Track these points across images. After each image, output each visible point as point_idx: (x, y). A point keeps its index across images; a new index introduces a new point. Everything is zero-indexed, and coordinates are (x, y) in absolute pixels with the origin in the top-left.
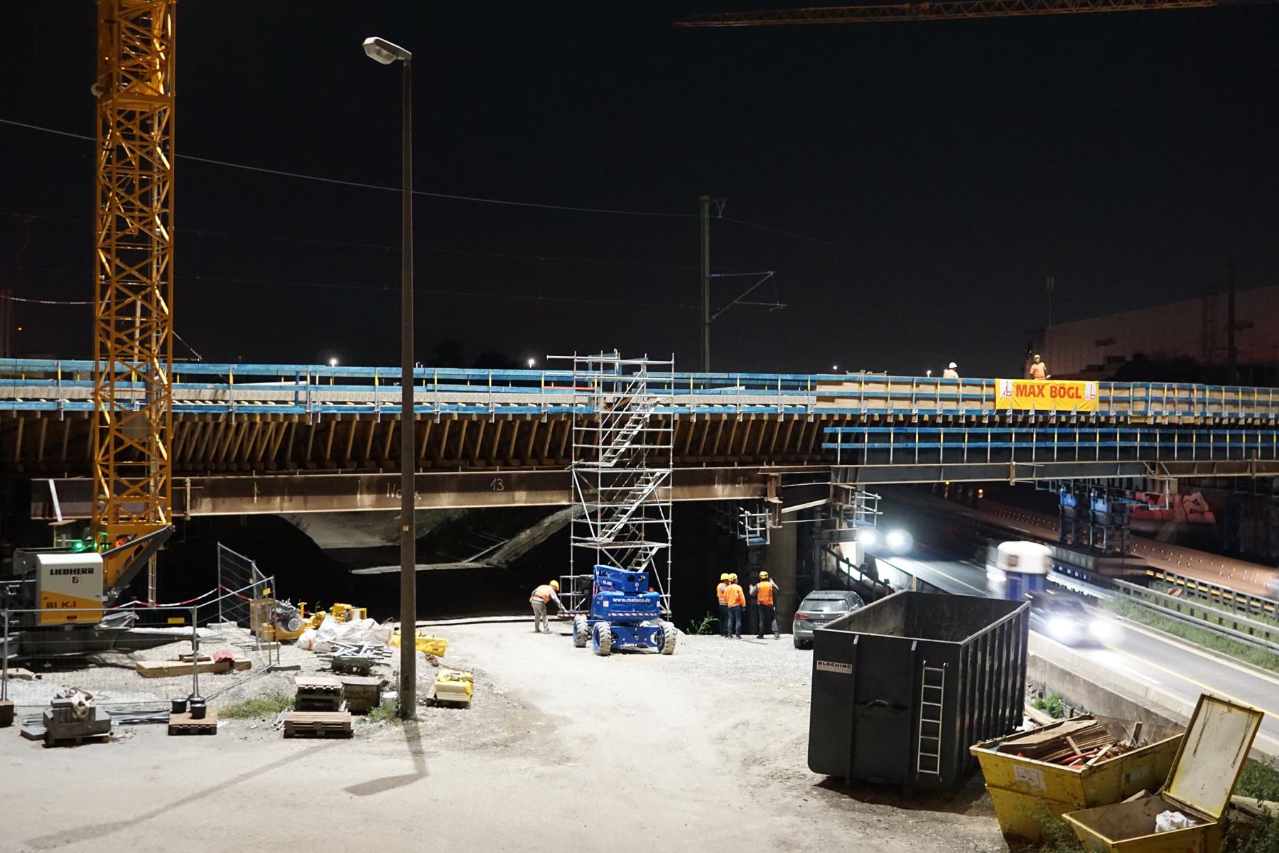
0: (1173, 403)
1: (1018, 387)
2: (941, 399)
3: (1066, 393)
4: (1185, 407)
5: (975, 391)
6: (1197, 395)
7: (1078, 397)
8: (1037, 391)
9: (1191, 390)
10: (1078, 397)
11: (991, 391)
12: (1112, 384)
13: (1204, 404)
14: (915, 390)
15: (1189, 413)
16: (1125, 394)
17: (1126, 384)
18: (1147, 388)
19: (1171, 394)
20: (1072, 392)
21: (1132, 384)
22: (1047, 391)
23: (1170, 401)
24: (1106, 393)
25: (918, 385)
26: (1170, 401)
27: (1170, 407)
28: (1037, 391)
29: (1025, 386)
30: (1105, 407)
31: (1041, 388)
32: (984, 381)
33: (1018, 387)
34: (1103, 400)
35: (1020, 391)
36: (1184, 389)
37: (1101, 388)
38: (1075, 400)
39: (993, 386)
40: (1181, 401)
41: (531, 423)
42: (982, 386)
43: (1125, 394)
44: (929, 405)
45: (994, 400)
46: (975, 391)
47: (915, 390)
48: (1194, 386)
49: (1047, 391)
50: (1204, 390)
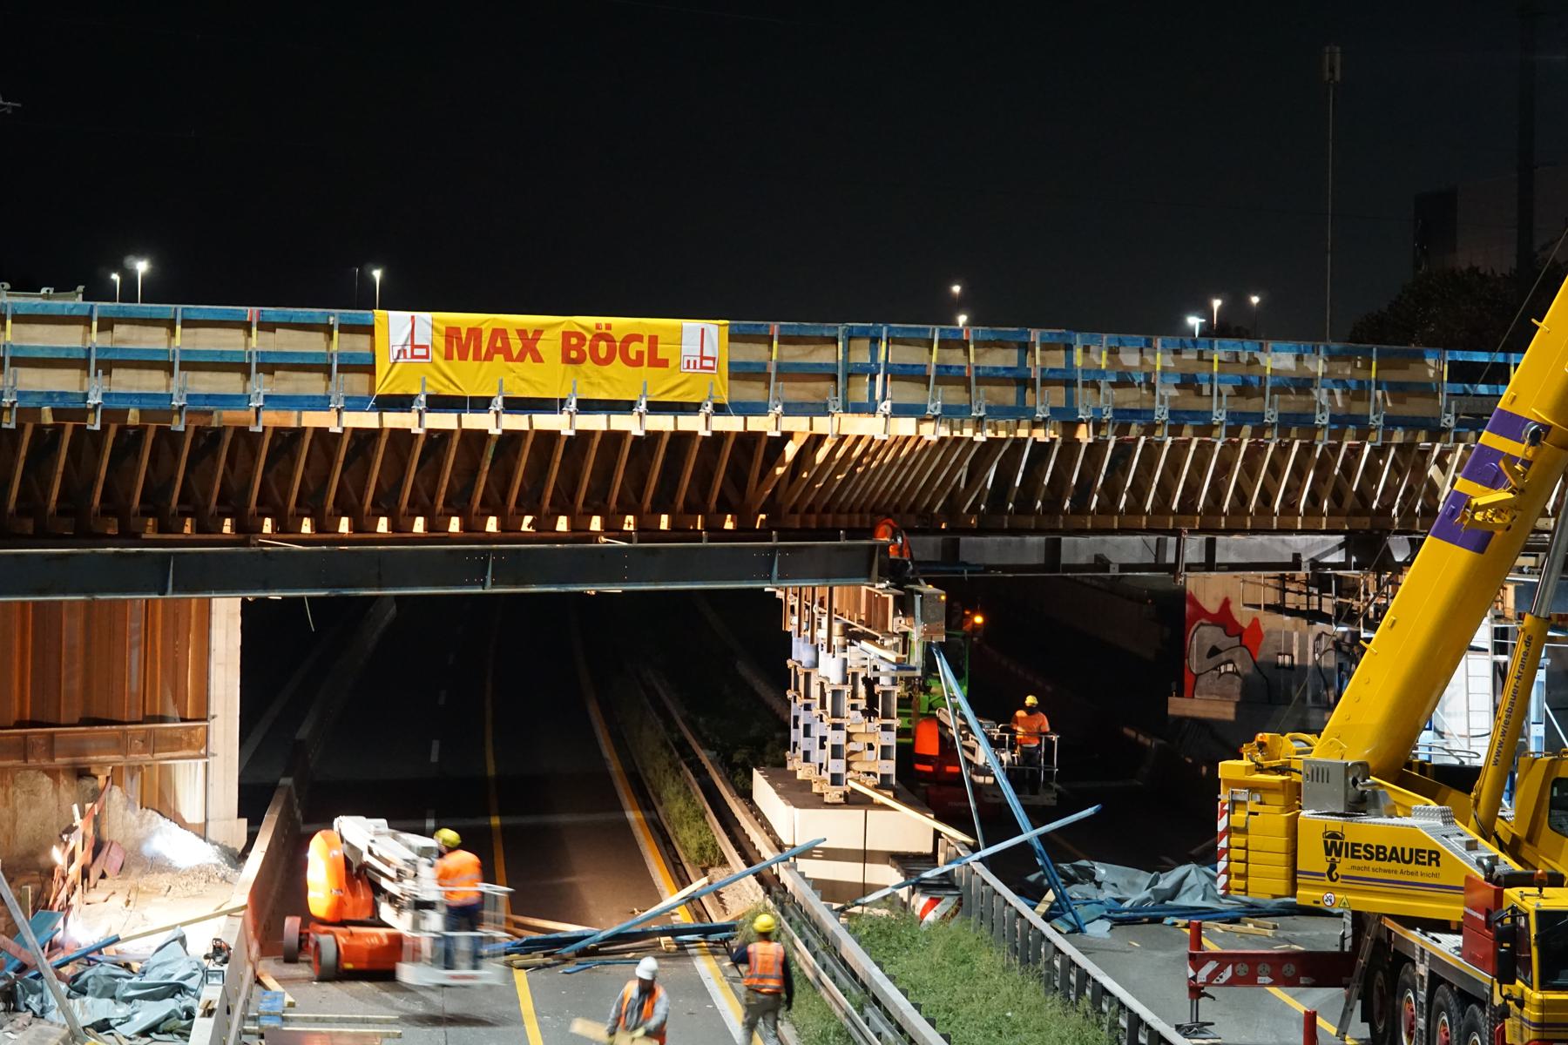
0: (965, 382)
1: (452, 334)
2: (185, 366)
3: (619, 350)
4: (1009, 395)
5: (312, 343)
6: (1038, 361)
7: (664, 363)
8: (516, 345)
9: (1026, 347)
10: (664, 363)
11: (360, 343)
12: (775, 328)
13: (1070, 383)
14: (96, 339)
15: (1020, 412)
16: (824, 356)
17: (826, 330)
18: (875, 341)
19: (955, 357)
21: (841, 328)
22: (550, 346)
23: (946, 376)
24: (753, 353)
25: (107, 325)
26: (946, 376)
27: (955, 395)
28: (516, 345)
29: (475, 333)
30: (752, 392)
31: (530, 342)
32: (335, 316)
33: (452, 334)
34: (740, 372)
35: (458, 345)
36: (1001, 344)
37: (733, 338)
38: (645, 369)
39: (369, 330)
40: (989, 378)
41: (58, 430)
42: (328, 330)
43: (824, 356)
44: (152, 382)
45: (370, 369)
46: (312, 343)
47: (96, 339)
48: (1035, 335)
49: (550, 346)
50: (1069, 348)
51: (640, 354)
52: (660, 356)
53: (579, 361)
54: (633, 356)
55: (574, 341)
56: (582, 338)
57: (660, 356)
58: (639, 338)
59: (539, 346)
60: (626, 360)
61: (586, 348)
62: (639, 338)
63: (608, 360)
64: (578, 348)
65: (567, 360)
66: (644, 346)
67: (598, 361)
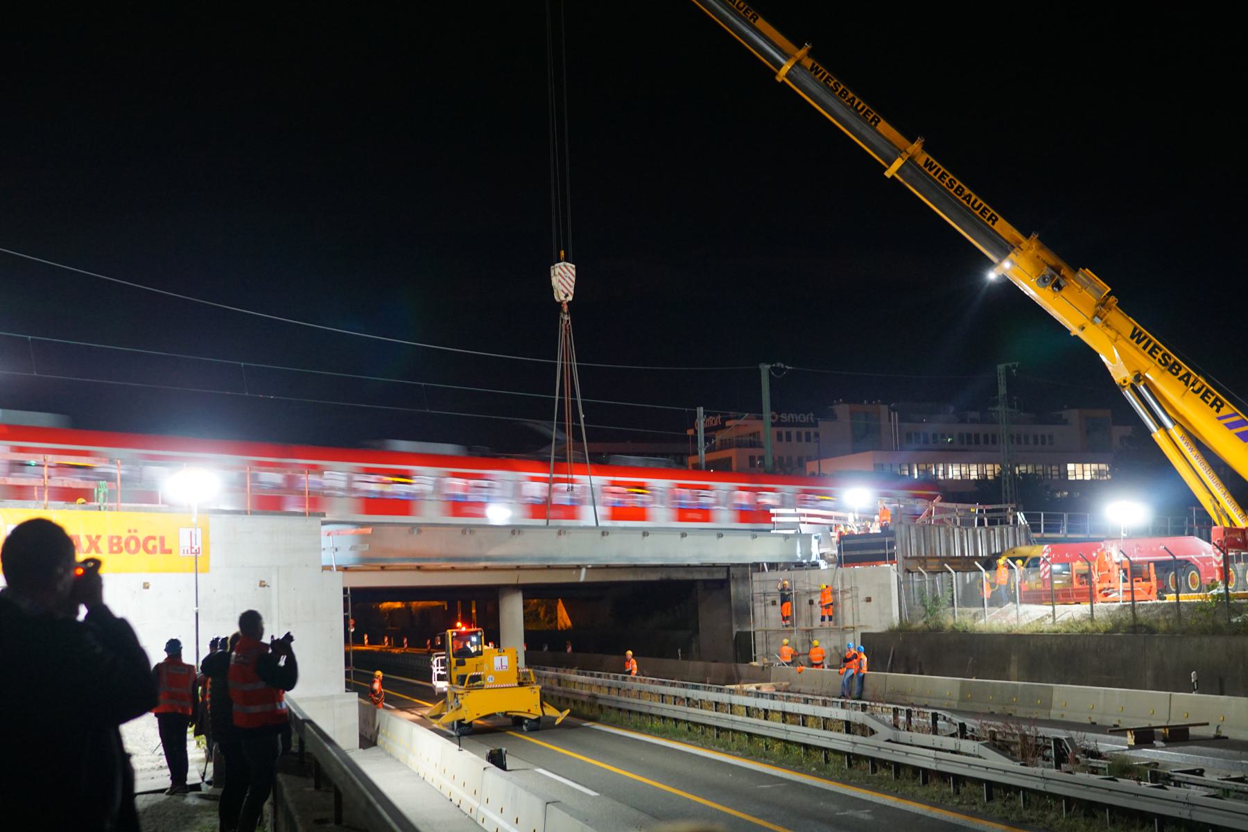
7: (170, 552)
10: (170, 552)
20: (151, 544)
38: (159, 556)
51: (154, 547)
52: (167, 547)
53: (120, 551)
54: (150, 547)
55: (115, 541)
56: (119, 538)
57: (167, 547)
58: (154, 538)
59: (100, 544)
60: (147, 551)
61: (123, 545)
62: (154, 538)
63: (136, 551)
64: (118, 544)
65: (111, 552)
66: (157, 543)
67: (129, 551)
